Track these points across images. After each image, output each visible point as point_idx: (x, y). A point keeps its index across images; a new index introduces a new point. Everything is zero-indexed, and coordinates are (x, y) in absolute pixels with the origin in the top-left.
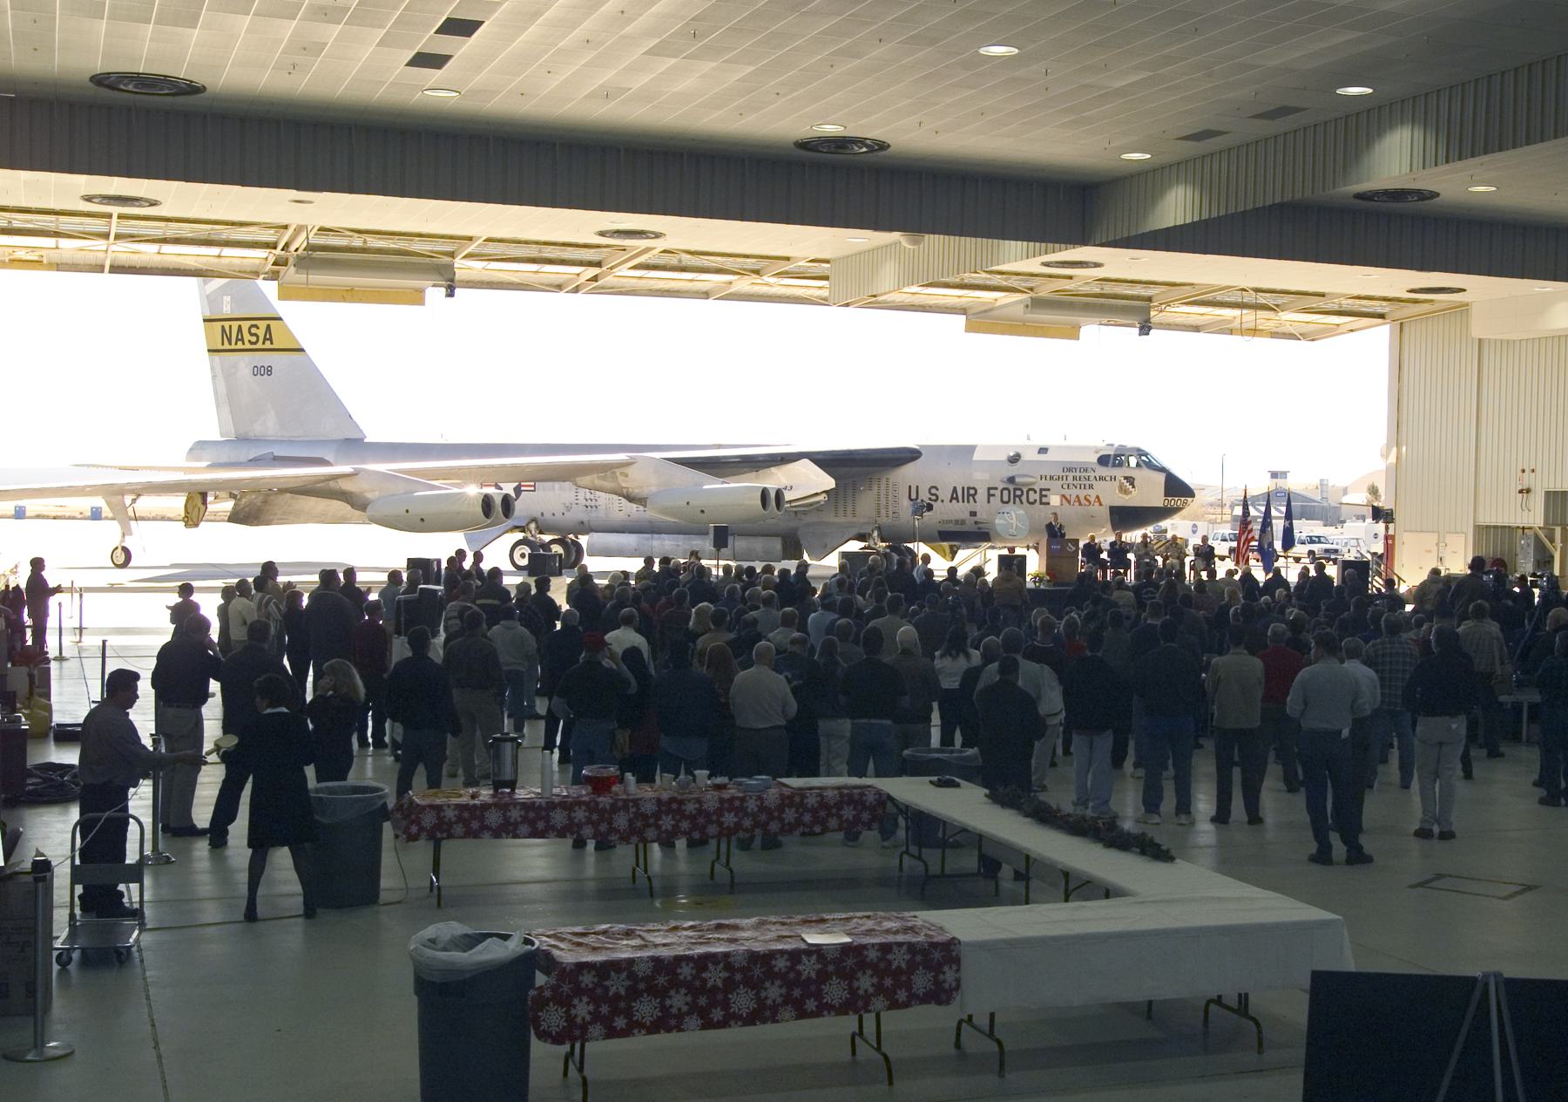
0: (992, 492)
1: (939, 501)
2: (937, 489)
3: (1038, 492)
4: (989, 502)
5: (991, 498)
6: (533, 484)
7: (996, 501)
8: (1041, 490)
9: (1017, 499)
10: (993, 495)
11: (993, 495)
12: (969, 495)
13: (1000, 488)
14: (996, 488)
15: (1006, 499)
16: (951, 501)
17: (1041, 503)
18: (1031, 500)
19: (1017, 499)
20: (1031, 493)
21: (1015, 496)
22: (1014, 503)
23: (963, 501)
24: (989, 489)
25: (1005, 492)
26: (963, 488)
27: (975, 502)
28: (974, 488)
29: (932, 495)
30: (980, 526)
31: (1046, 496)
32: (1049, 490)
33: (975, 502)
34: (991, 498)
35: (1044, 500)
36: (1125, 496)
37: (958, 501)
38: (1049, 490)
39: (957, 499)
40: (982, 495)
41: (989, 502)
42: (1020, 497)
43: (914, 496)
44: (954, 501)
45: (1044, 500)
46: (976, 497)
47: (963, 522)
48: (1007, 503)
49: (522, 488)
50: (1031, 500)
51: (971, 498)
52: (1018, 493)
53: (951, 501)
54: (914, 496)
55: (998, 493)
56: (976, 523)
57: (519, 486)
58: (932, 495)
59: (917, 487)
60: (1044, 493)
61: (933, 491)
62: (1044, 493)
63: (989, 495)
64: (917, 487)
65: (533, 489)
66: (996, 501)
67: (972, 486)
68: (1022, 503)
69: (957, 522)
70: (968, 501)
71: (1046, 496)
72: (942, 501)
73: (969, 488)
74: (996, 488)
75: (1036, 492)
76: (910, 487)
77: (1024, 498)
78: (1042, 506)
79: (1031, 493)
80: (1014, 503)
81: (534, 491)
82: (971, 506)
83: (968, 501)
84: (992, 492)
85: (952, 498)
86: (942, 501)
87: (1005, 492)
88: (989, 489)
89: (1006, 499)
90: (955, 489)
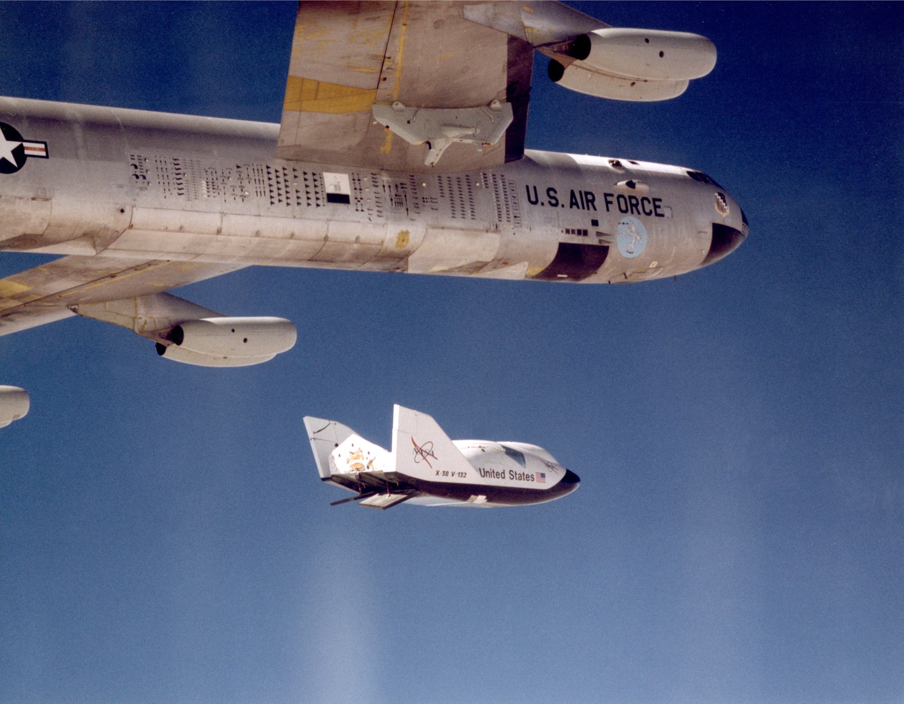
0: (609, 199)
1: (560, 205)
2: (556, 192)
3: (651, 201)
4: (608, 210)
5: (609, 205)
6: (43, 146)
7: (614, 207)
8: (655, 200)
9: (634, 209)
10: (611, 203)
11: (611, 203)
12: (588, 201)
13: (616, 196)
14: (612, 195)
15: (624, 208)
16: (571, 207)
17: (657, 215)
18: (647, 211)
19: (634, 209)
20: (646, 202)
21: (632, 205)
22: (632, 213)
23: (583, 208)
24: (606, 195)
25: (622, 200)
26: (580, 192)
27: (595, 209)
28: (591, 193)
29: (551, 197)
30: (603, 238)
31: (659, 207)
32: (660, 200)
33: (595, 209)
34: (609, 205)
35: (659, 211)
36: (721, 213)
37: (578, 207)
38: (660, 200)
39: (576, 204)
40: (600, 202)
41: (608, 210)
42: (636, 205)
43: (533, 199)
44: (575, 207)
45: (659, 211)
46: (596, 203)
47: (585, 233)
48: (626, 211)
49: (27, 152)
50: (647, 211)
51: (590, 204)
52: (634, 201)
53: (571, 207)
54: (533, 199)
55: (614, 199)
56: (599, 234)
57: (22, 145)
58: (551, 197)
59: (535, 188)
60: (657, 203)
61: (552, 193)
62: (657, 203)
63: (608, 203)
64: (535, 188)
65: (44, 154)
66: (614, 207)
67: (588, 190)
68: (639, 213)
69: (579, 232)
70: (588, 209)
71: (659, 207)
72: (563, 206)
73: (587, 193)
74: (612, 195)
75: (649, 202)
76: (527, 187)
77: (640, 207)
78: (657, 218)
79: (646, 202)
80: (632, 213)
81: (47, 157)
82: (592, 214)
83: (588, 209)
84: (609, 199)
85: (572, 205)
86: (563, 206)
87: (622, 200)
88: (606, 195)
89: (624, 208)
90: (572, 193)
